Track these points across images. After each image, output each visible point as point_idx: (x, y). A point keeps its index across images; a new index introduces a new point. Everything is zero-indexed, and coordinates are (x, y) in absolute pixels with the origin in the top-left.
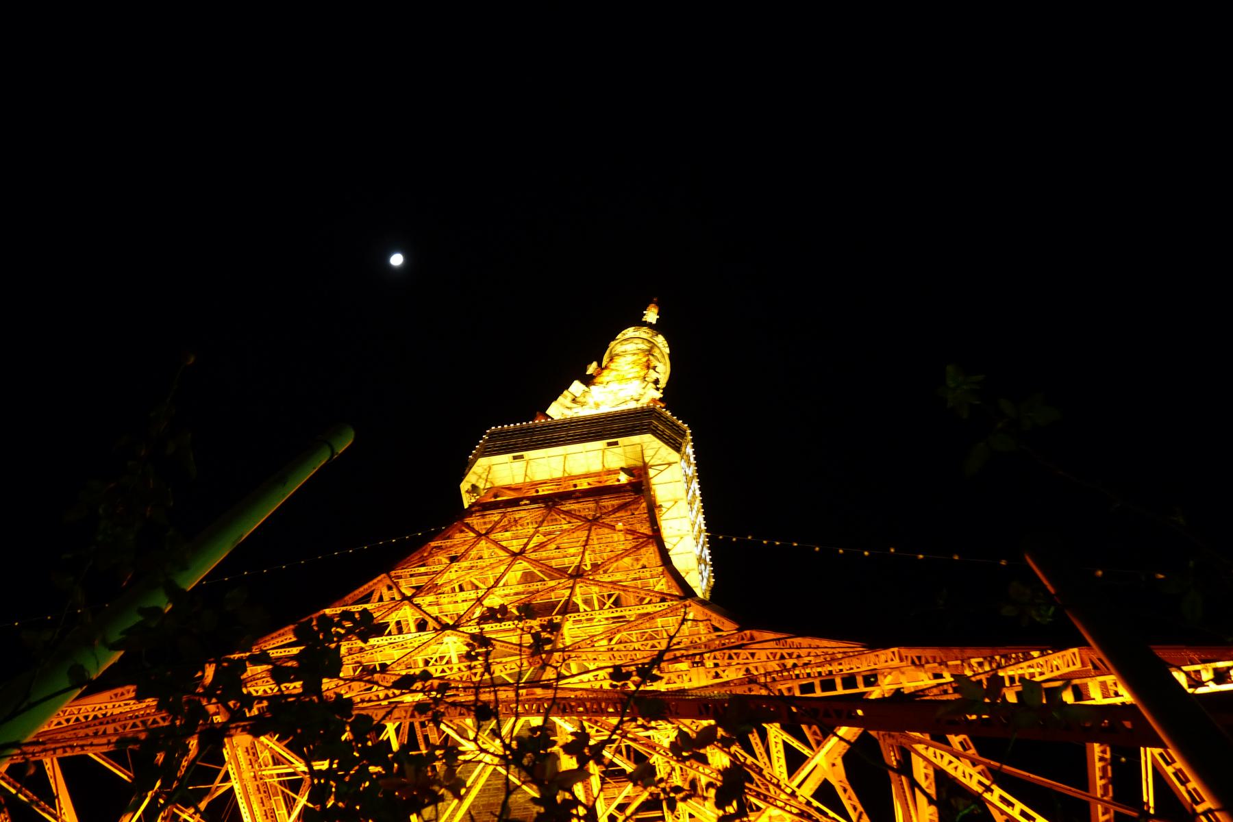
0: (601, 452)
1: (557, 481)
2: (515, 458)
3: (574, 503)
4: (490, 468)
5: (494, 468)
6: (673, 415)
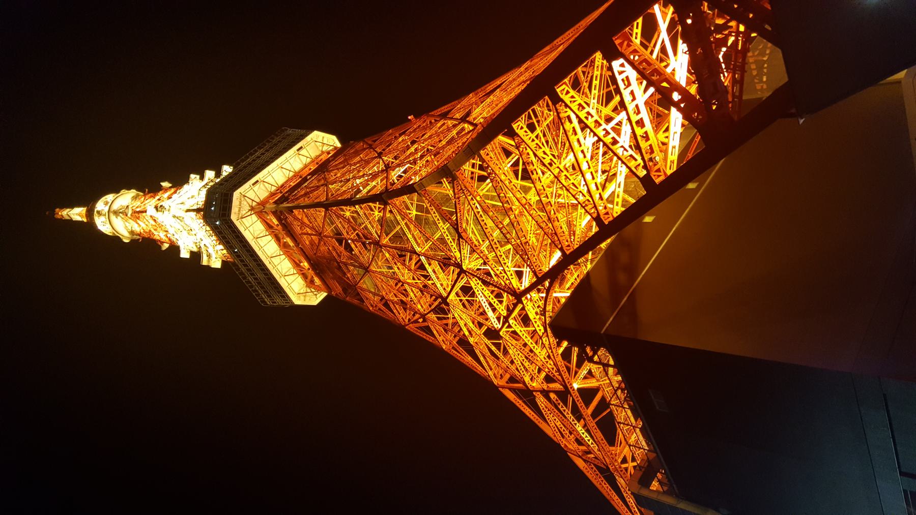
4: (298, 294)
5: (297, 291)
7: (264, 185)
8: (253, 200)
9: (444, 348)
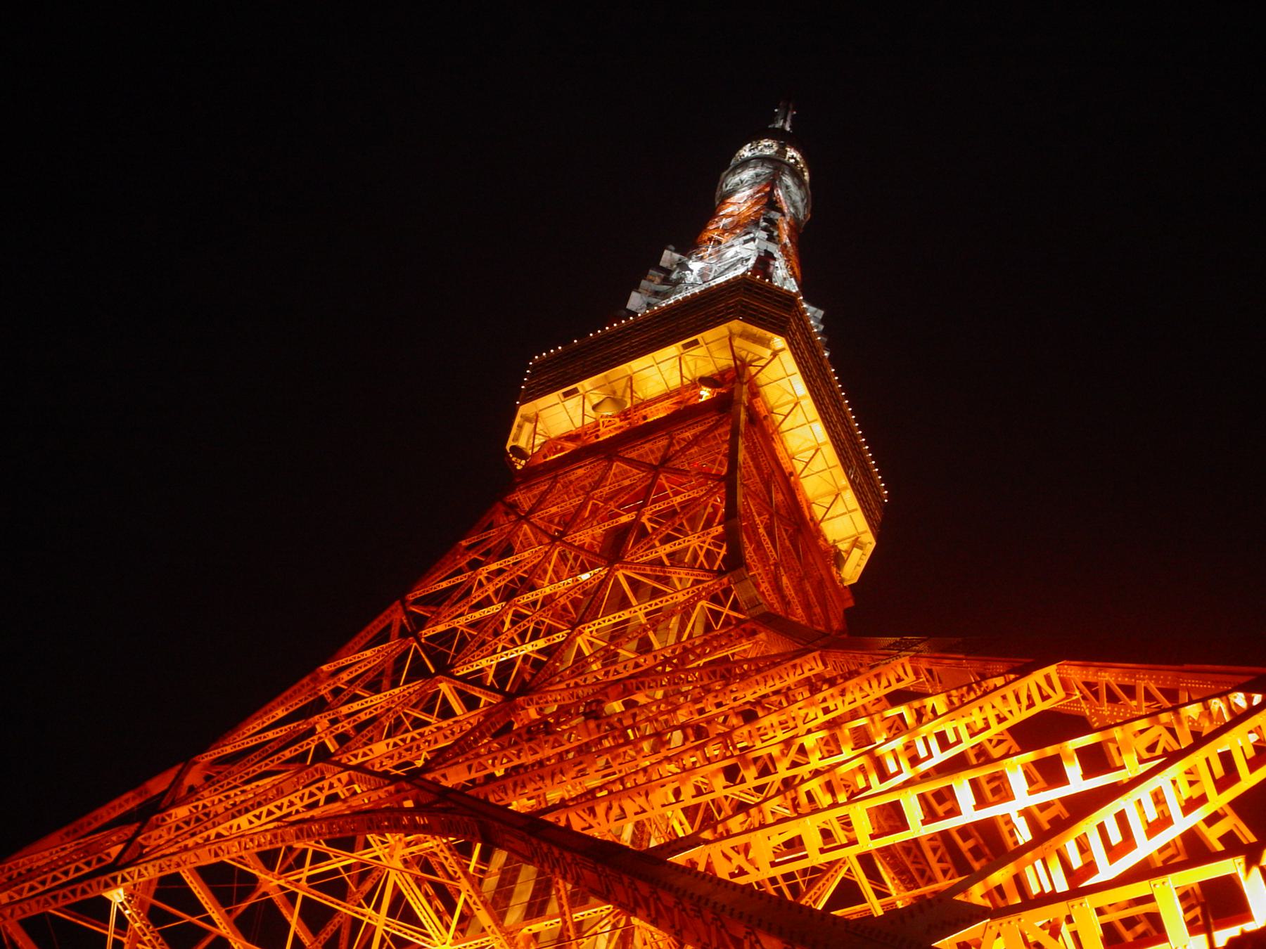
2: (566, 395)
3: (642, 444)
5: (543, 414)
7: (788, 403)
8: (763, 367)
9: (324, 668)
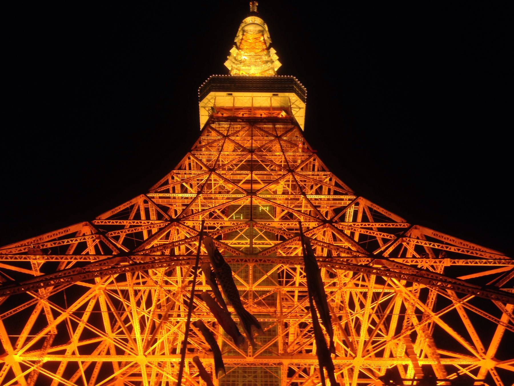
0: (269, 99)
1: (249, 109)
6: (301, 83)
